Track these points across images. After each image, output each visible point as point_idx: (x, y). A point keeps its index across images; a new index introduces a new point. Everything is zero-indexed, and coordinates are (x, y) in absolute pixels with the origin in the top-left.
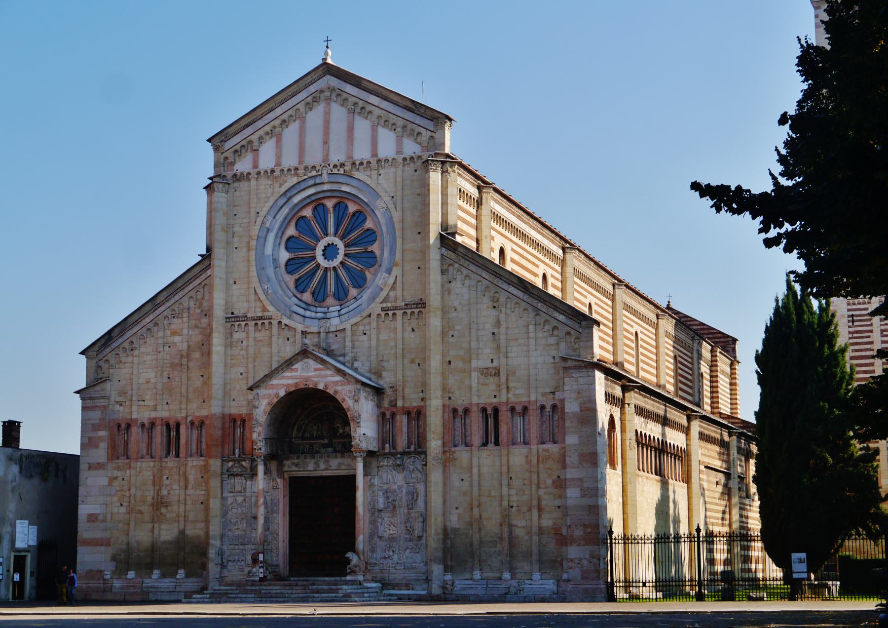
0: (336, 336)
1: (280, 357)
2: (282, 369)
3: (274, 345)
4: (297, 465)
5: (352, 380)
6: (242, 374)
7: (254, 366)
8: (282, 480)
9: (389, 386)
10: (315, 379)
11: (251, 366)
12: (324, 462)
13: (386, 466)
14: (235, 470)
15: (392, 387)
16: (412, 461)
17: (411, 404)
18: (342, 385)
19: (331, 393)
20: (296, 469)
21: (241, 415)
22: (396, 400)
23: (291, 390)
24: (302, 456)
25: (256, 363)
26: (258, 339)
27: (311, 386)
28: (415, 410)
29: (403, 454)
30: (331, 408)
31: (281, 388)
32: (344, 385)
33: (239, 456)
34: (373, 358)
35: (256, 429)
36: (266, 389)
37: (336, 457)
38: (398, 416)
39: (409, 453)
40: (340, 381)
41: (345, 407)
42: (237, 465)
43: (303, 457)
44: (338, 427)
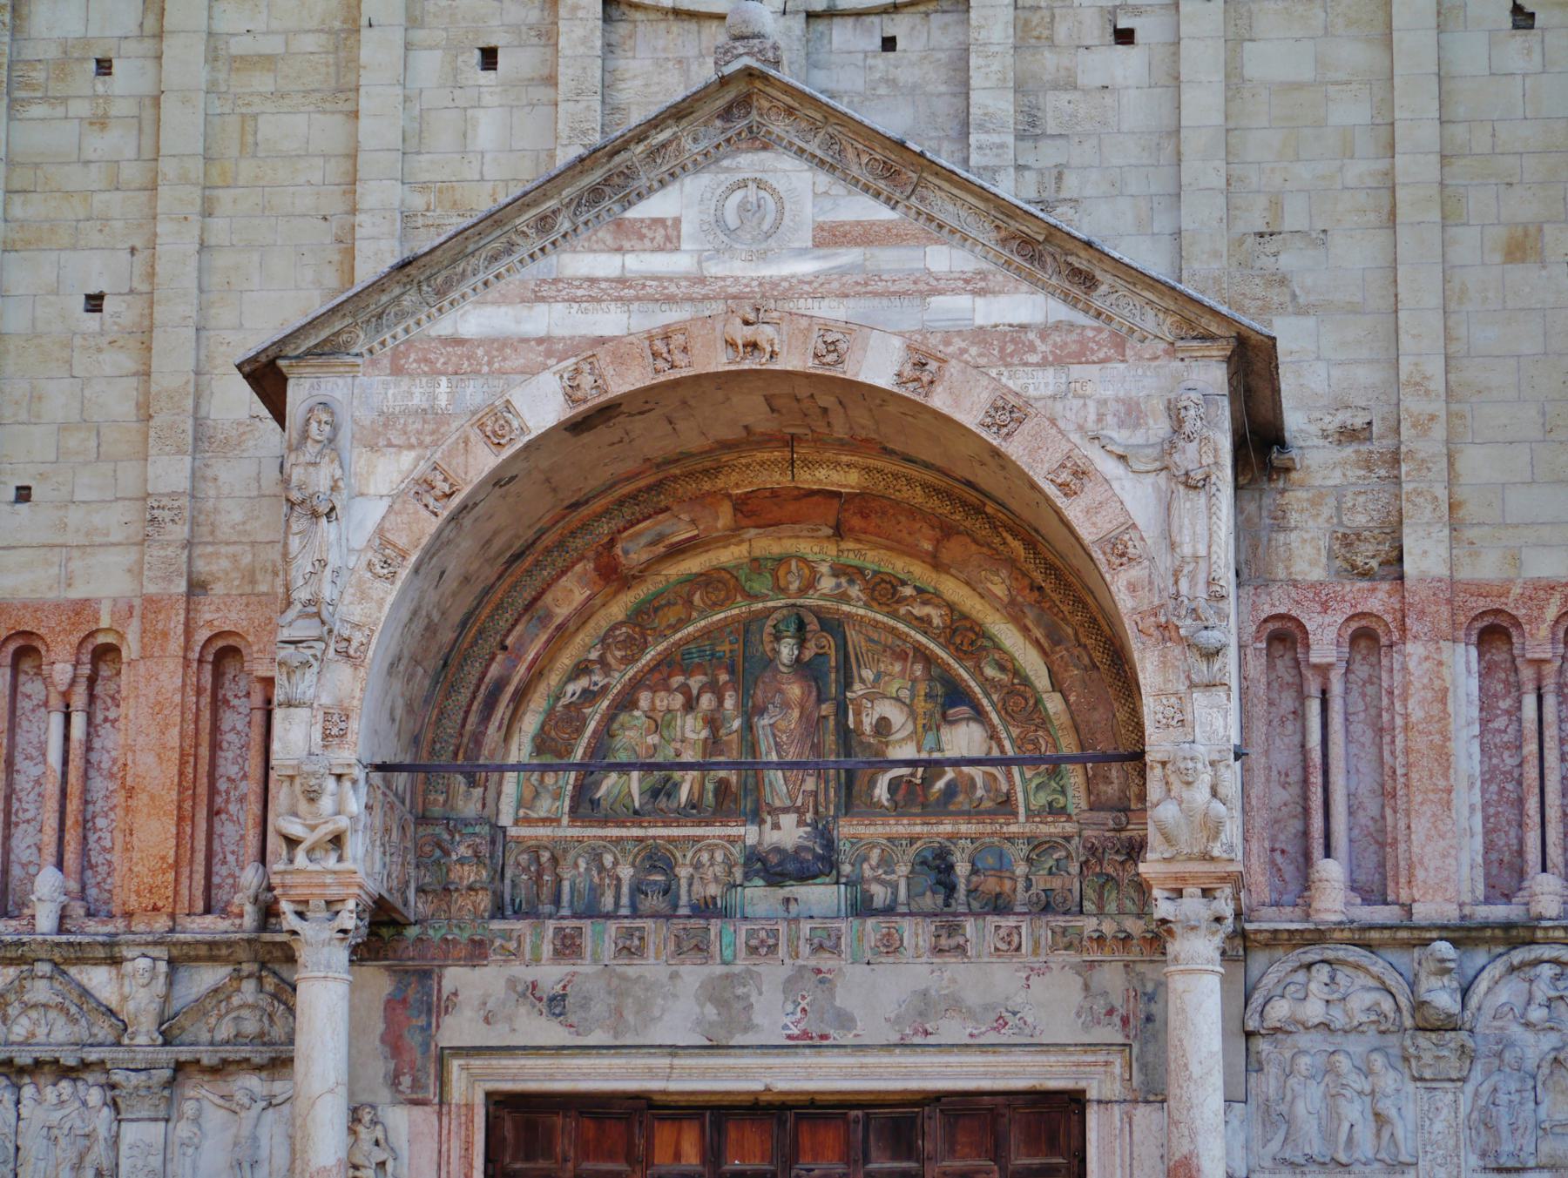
0: (889, 44)
1: (424, 187)
2: (544, 224)
3: (378, 98)
4: (556, 1005)
5: (1149, 321)
6: (94, 302)
7: (203, 247)
8: (425, 1117)
9: (1333, 422)
10: (832, 310)
11: (177, 244)
12: (790, 985)
13: (1325, 1026)
14: (20, 1030)
15: (1348, 435)
16: (1543, 990)
17: (1516, 560)
18: (1058, 361)
19: (970, 417)
20: (554, 1033)
21: (82, 609)
22: (1393, 532)
23: (618, 386)
24: (601, 938)
25: (218, 224)
26: (238, 46)
27: (790, 362)
28: (1552, 612)
29: (1465, 935)
30: (827, 584)
31: (531, 372)
32: (1081, 356)
33: (63, 917)
34: (1202, 213)
35: (305, 685)
36: (397, 371)
37: (891, 946)
38: (1414, 649)
39: (1516, 935)
40: (1044, 332)
41: (1087, 533)
42: (40, 991)
43: (608, 949)
44: (883, 726)
